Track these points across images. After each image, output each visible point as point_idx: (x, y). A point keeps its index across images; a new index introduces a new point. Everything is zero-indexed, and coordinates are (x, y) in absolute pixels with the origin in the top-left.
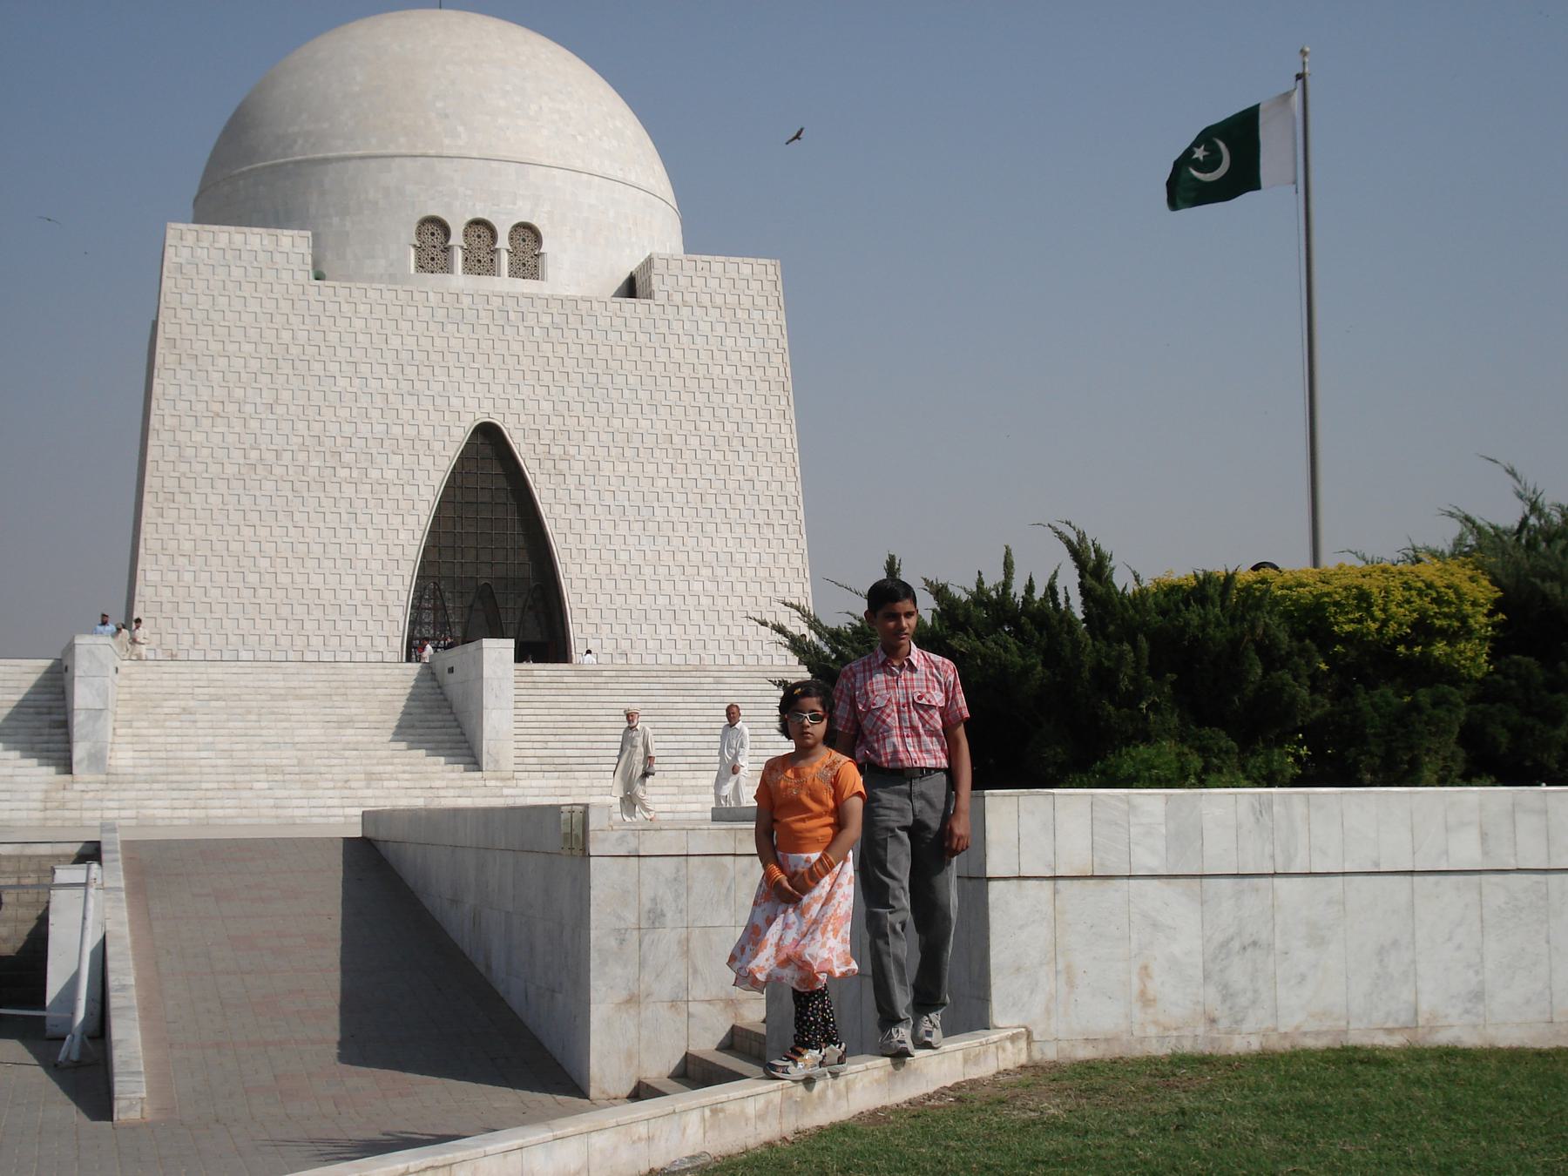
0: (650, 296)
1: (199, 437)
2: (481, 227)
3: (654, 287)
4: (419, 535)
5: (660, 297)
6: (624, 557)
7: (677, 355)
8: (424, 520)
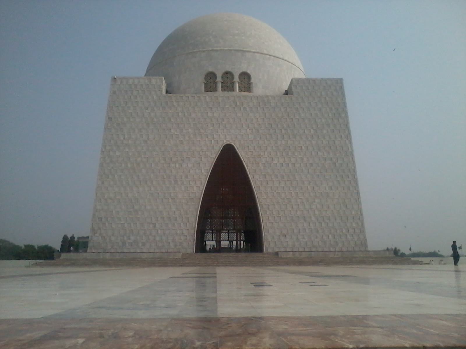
0: (292, 94)
1: (118, 153)
2: (228, 75)
4: (201, 188)
6: (283, 195)
7: (303, 115)
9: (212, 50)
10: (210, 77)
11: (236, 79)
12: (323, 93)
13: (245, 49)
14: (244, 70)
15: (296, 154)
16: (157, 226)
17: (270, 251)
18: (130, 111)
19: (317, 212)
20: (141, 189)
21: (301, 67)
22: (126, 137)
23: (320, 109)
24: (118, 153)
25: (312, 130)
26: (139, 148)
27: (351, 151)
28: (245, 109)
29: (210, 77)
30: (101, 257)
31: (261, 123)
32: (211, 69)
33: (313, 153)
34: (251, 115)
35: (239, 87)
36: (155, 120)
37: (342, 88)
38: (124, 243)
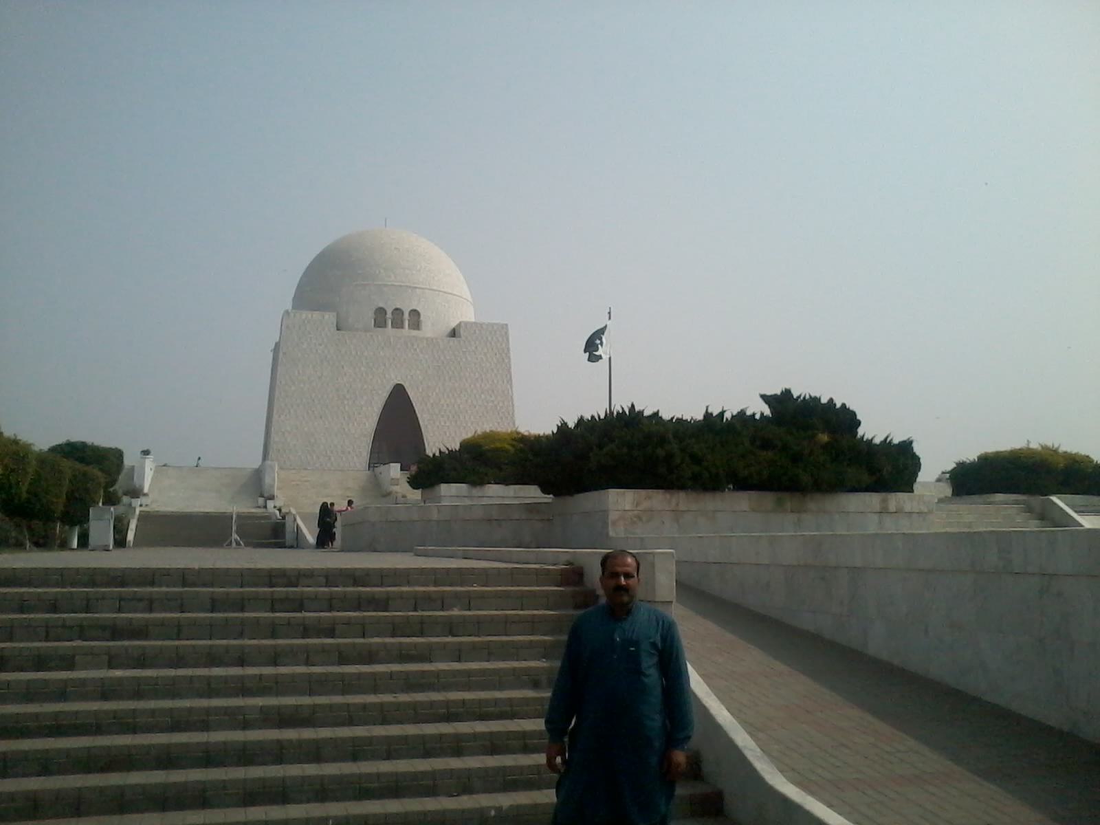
0: (460, 337)
2: (398, 311)
5: (463, 338)
11: (406, 315)
14: (414, 308)
21: (470, 299)
32: (381, 305)
34: (421, 355)
35: (409, 325)
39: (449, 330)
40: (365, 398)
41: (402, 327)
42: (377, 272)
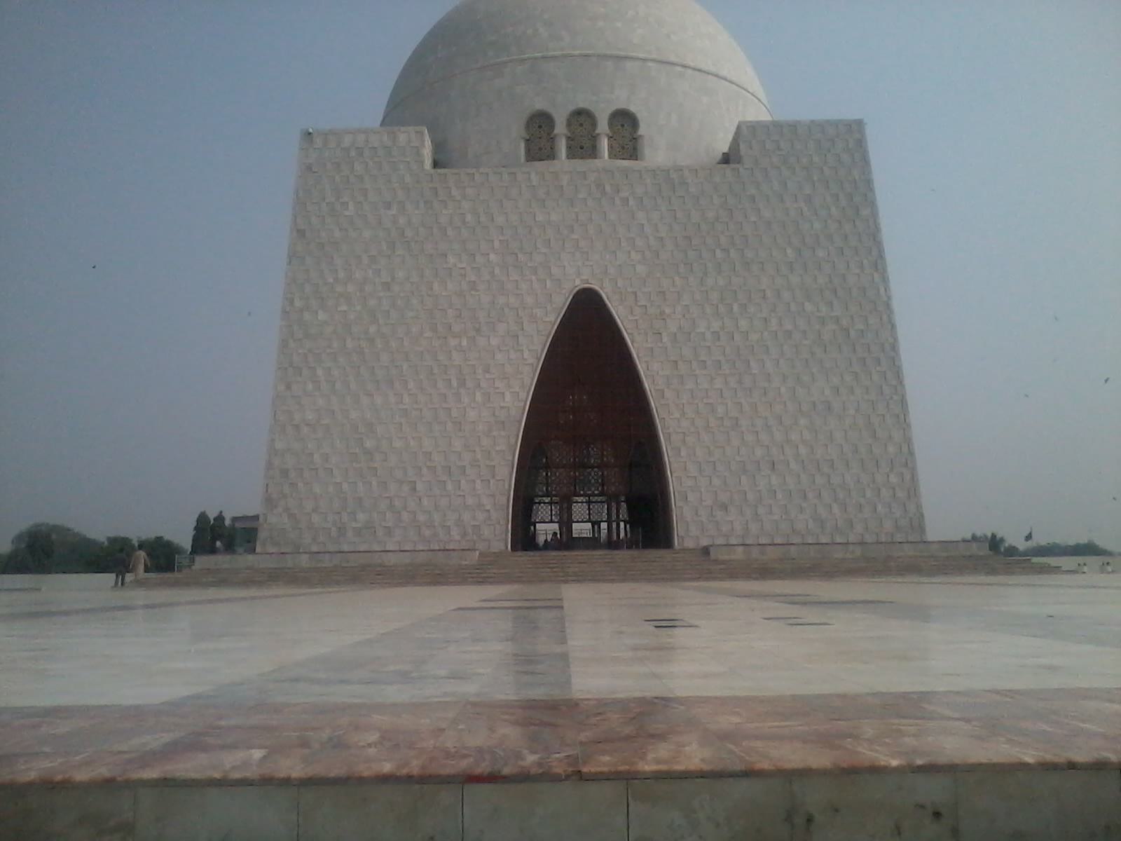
1: (322, 316)
2: (582, 117)
3: (742, 153)
4: (523, 395)
6: (720, 410)
8: (527, 381)
9: (543, 57)
10: (540, 123)
11: (603, 126)
12: (816, 159)
13: (622, 53)
15: (752, 309)
16: (419, 486)
17: (689, 544)
18: (347, 213)
19: (803, 450)
20: (379, 400)
21: (761, 94)
22: (341, 275)
23: (809, 200)
24: (322, 316)
25: (789, 251)
26: (372, 302)
27: (885, 299)
28: (625, 201)
29: (540, 123)
30: (290, 564)
31: (663, 235)
32: (540, 104)
33: (793, 307)
34: (641, 215)
36: (409, 233)
37: (861, 143)
38: (342, 531)
39: (719, 156)
40: (501, 328)
41: (593, 152)
42: (530, 32)
